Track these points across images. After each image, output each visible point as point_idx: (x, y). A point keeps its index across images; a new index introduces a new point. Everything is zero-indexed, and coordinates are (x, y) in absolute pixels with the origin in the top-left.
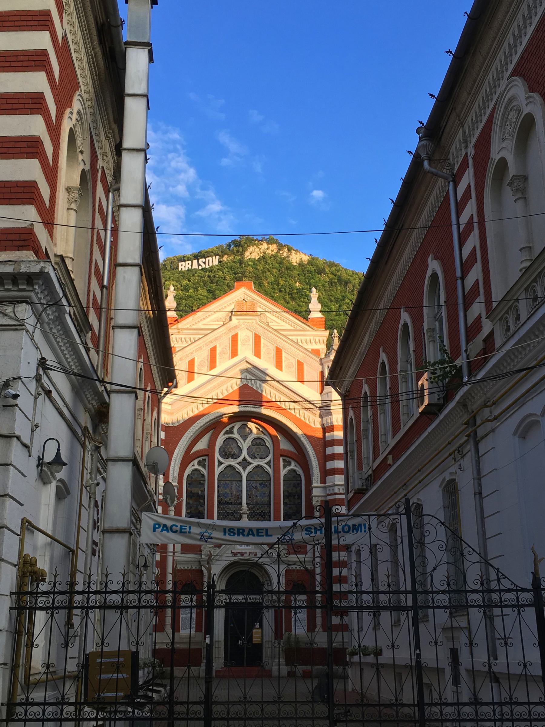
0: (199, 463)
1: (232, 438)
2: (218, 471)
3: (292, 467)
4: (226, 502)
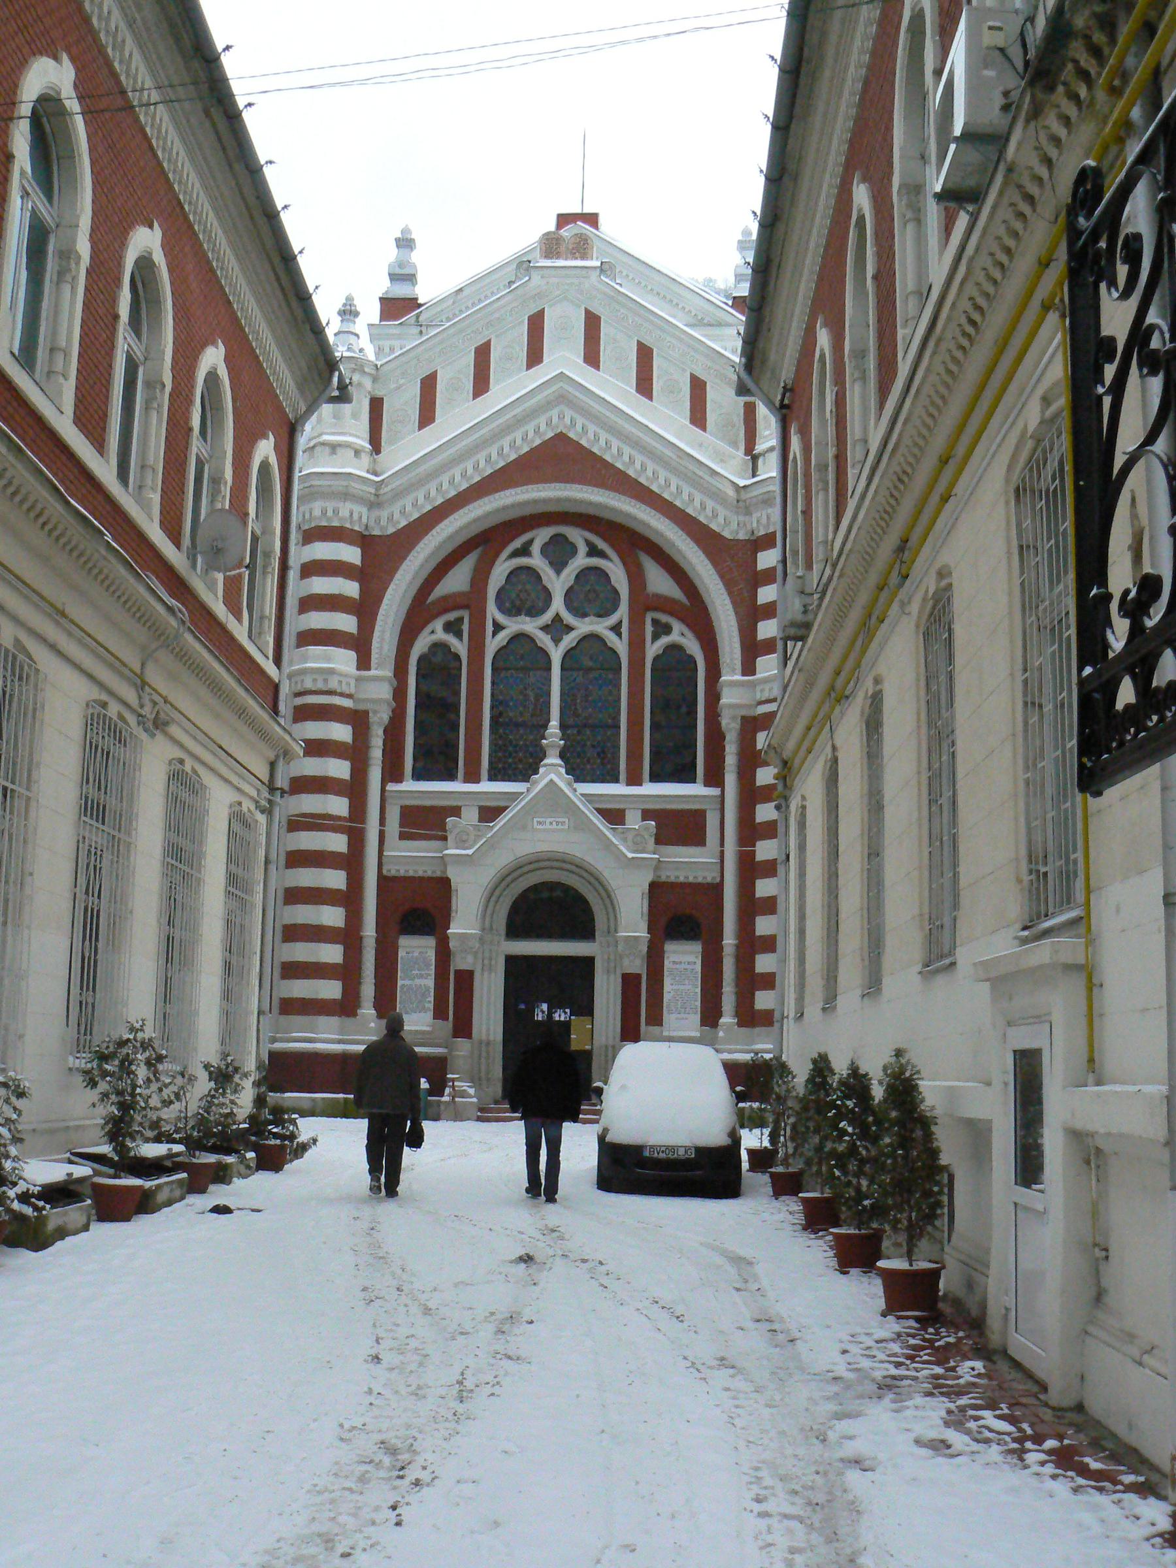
1: (529, 569)
2: (493, 644)
3: (674, 637)
4: (511, 720)
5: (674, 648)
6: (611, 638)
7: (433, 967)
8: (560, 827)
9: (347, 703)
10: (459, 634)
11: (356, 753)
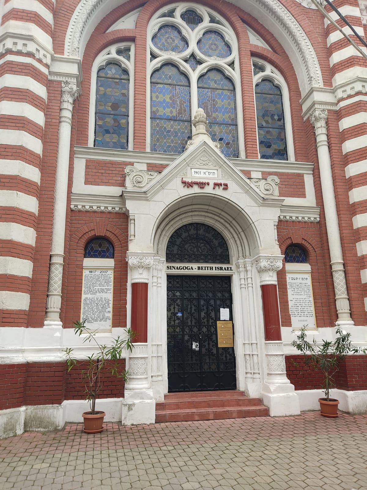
0: (119, 52)
5: (267, 80)
6: (229, 71)
7: (112, 284)
8: (211, 176)
9: (45, 70)
10: (128, 59)
11: (51, 108)
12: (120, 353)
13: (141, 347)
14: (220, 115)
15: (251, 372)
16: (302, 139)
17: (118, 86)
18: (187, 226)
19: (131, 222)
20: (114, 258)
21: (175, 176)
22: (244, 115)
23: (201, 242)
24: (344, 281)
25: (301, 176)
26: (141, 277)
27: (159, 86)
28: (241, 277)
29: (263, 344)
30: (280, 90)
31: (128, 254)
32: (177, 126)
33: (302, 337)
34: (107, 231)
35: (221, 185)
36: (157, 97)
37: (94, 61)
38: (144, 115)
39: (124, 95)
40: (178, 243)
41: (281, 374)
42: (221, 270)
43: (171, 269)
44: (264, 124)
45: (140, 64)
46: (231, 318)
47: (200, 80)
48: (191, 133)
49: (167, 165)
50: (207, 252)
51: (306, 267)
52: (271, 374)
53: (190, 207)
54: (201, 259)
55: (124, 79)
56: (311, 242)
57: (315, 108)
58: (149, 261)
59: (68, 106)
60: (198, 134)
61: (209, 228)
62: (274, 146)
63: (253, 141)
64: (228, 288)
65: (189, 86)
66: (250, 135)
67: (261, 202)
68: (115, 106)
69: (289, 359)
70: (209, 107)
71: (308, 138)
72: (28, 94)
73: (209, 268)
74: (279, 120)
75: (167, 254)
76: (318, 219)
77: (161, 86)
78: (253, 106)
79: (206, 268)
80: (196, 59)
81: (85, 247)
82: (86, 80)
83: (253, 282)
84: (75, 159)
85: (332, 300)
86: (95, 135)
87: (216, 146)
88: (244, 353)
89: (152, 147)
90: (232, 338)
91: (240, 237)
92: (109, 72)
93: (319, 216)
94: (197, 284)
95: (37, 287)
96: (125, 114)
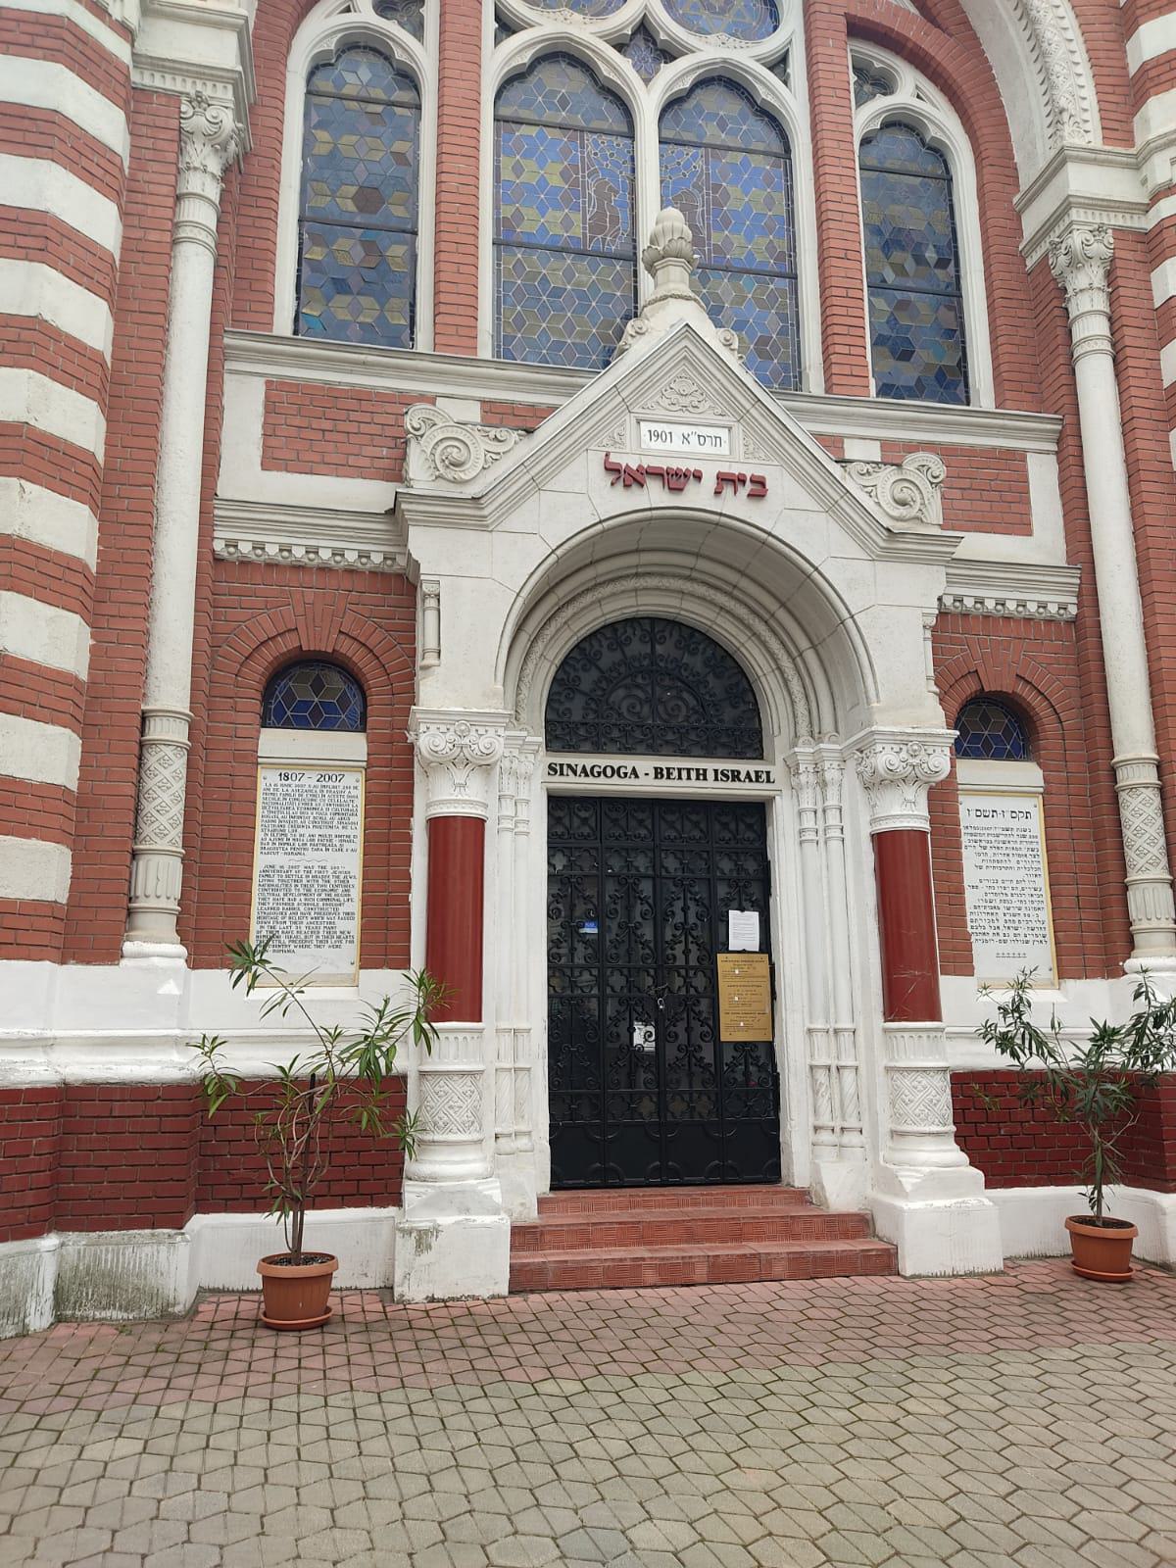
5: (901, 123)
6: (768, 87)
7: (359, 819)
8: (708, 448)
10: (418, 31)
12: (388, 1054)
13: (461, 1036)
14: (738, 240)
15: (831, 1124)
16: (1022, 332)
17: (382, 129)
18: (617, 626)
19: (427, 605)
20: (364, 730)
21: (581, 446)
22: (821, 242)
23: (667, 682)
24: (1160, 821)
25: (1017, 458)
26: (460, 797)
27: (524, 130)
28: (804, 806)
29: (878, 1033)
30: (945, 163)
31: (418, 716)
32: (586, 274)
33: (1016, 1008)
34: (342, 637)
35: (743, 482)
36: (518, 170)
37: (293, 34)
38: (472, 230)
39: (400, 158)
40: (585, 686)
41: (938, 1134)
42: (733, 780)
43: (562, 774)
44: (890, 277)
45: (458, 51)
46: (766, 945)
47: (669, 116)
48: (636, 302)
49: (552, 409)
50: (687, 721)
51: (1027, 774)
52: (903, 1134)
53: (632, 560)
54: (667, 742)
55: (401, 105)
56: (1048, 688)
57: (1071, 223)
58: (492, 741)
59: (203, 184)
60: (665, 298)
61: (692, 636)
62: (923, 356)
63: (853, 331)
64: (757, 845)
65: (631, 135)
66: (843, 311)
67: (882, 544)
68: (369, 198)
69: (966, 1087)
70: (699, 210)
71: (1041, 327)
72: (56, 130)
73: (693, 774)
74: (942, 263)
75: (546, 721)
76: (1073, 610)
77: (533, 131)
78: (853, 209)
79: (684, 774)
80: (654, 43)
81: (266, 689)
82: (267, 101)
83: (846, 824)
84: (226, 376)
85: (1114, 888)
86: (298, 299)
87: (728, 344)
88: (808, 1061)
89: (499, 346)
90: (768, 1010)
91: (801, 666)
92: (350, 78)
93: (1074, 600)
94: (650, 827)
95: (94, 822)
96: (403, 227)
